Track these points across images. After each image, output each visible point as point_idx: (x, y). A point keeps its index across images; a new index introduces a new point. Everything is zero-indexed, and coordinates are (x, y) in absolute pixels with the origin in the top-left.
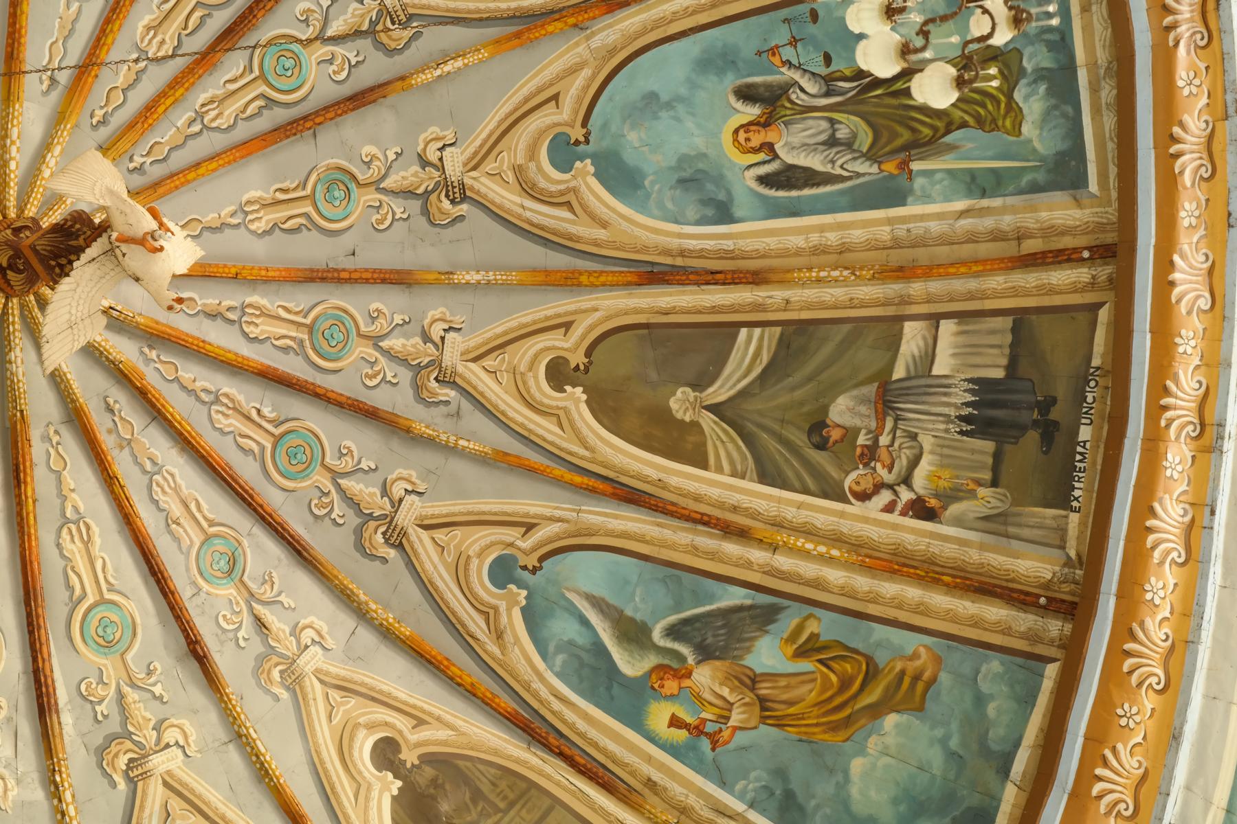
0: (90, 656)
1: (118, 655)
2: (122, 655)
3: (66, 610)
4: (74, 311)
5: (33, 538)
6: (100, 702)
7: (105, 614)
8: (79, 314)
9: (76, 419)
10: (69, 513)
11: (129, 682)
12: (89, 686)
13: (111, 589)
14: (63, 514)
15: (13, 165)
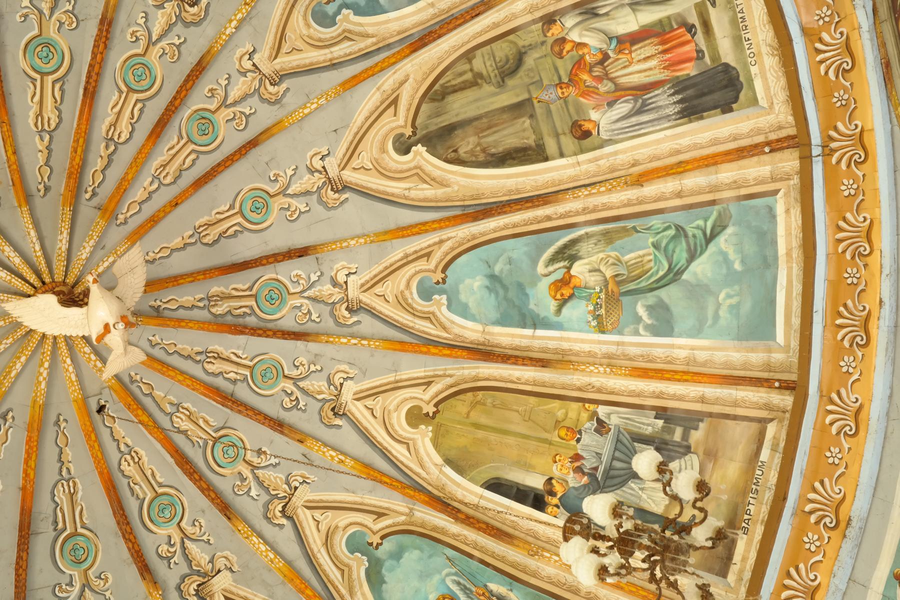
0: (62, 42)
1: (44, 36)
2: (40, 35)
3: (69, 77)
4: (132, 279)
5: (84, 130)
6: (68, 11)
7: (44, 66)
8: (129, 277)
9: (27, 198)
10: (47, 138)
11: (43, 16)
12: (71, 24)
13: (33, 80)
14: (51, 138)
15: (46, 365)
